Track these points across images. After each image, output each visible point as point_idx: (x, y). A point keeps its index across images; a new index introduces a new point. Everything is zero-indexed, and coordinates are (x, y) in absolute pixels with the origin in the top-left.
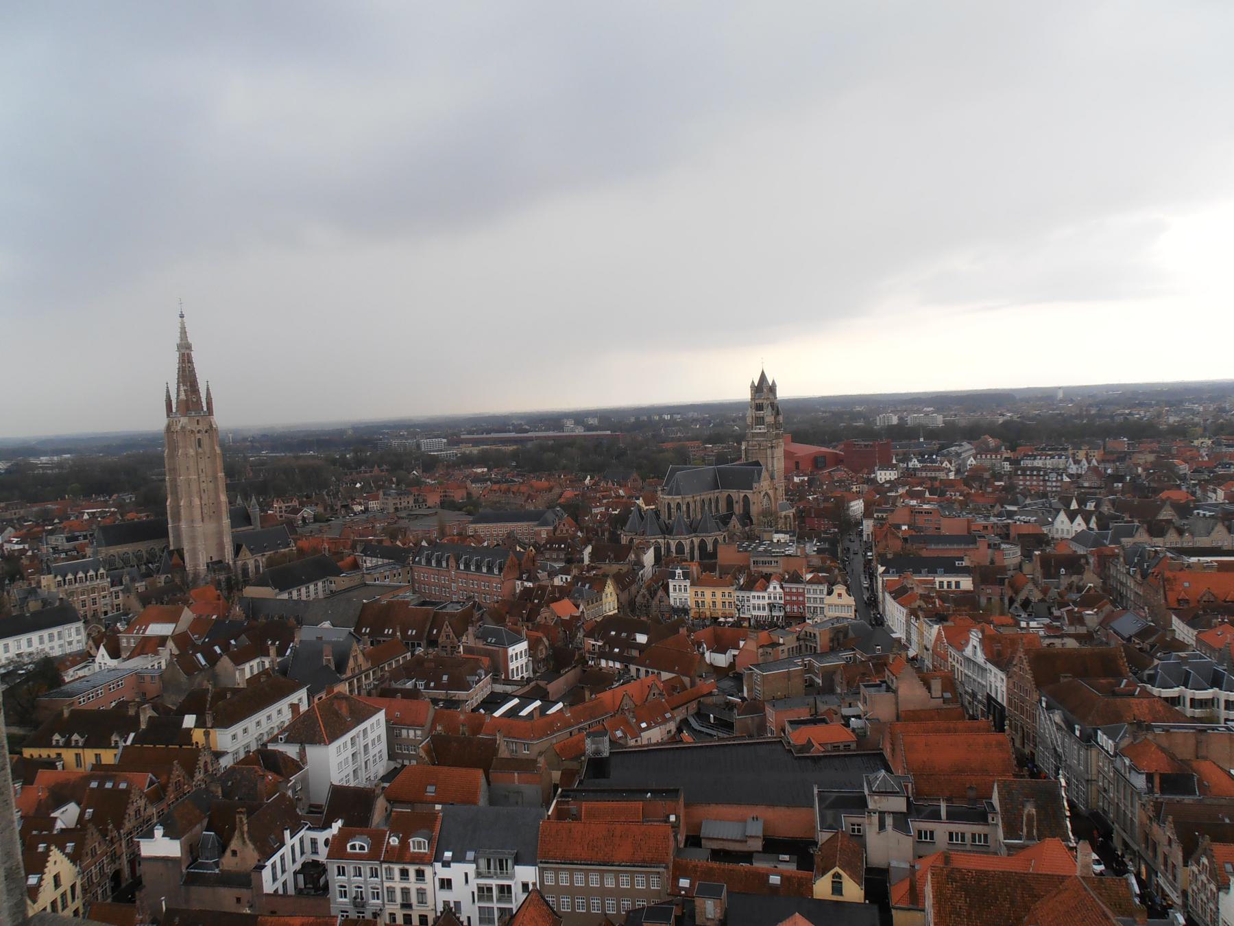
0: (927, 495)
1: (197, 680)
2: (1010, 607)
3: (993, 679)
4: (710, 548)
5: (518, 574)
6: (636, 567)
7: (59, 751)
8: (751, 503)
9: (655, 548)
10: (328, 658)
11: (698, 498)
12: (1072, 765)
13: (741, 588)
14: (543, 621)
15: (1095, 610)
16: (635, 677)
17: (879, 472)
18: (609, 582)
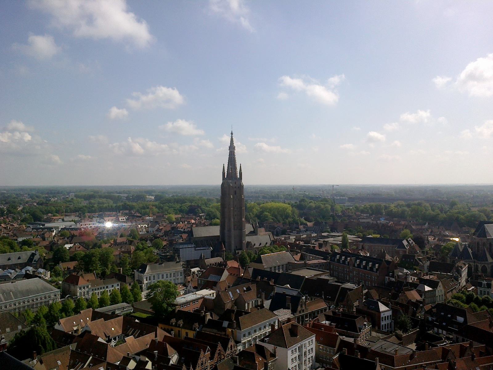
1: (229, 305)
7: (172, 327)
18: (440, 284)
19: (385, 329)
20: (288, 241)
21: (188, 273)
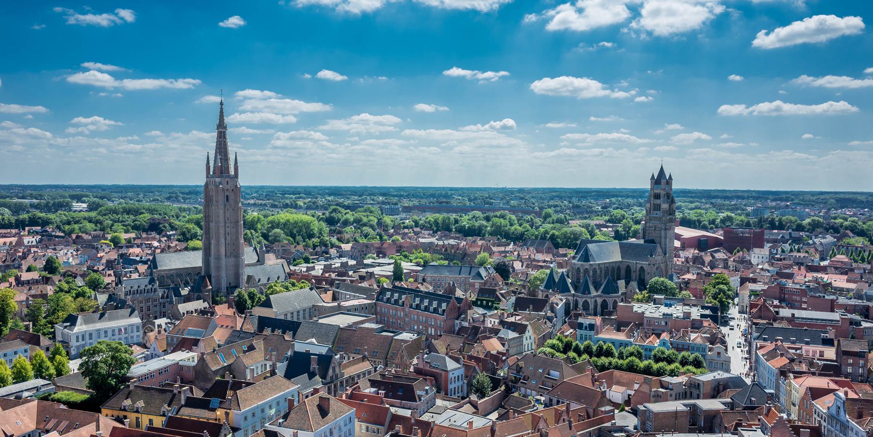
4: (610, 306)
5: (456, 315)
7: (125, 413)
8: (646, 273)
10: (314, 366)
11: (603, 266)
18: (529, 327)
19: (455, 394)
20: (313, 273)
21: (150, 327)
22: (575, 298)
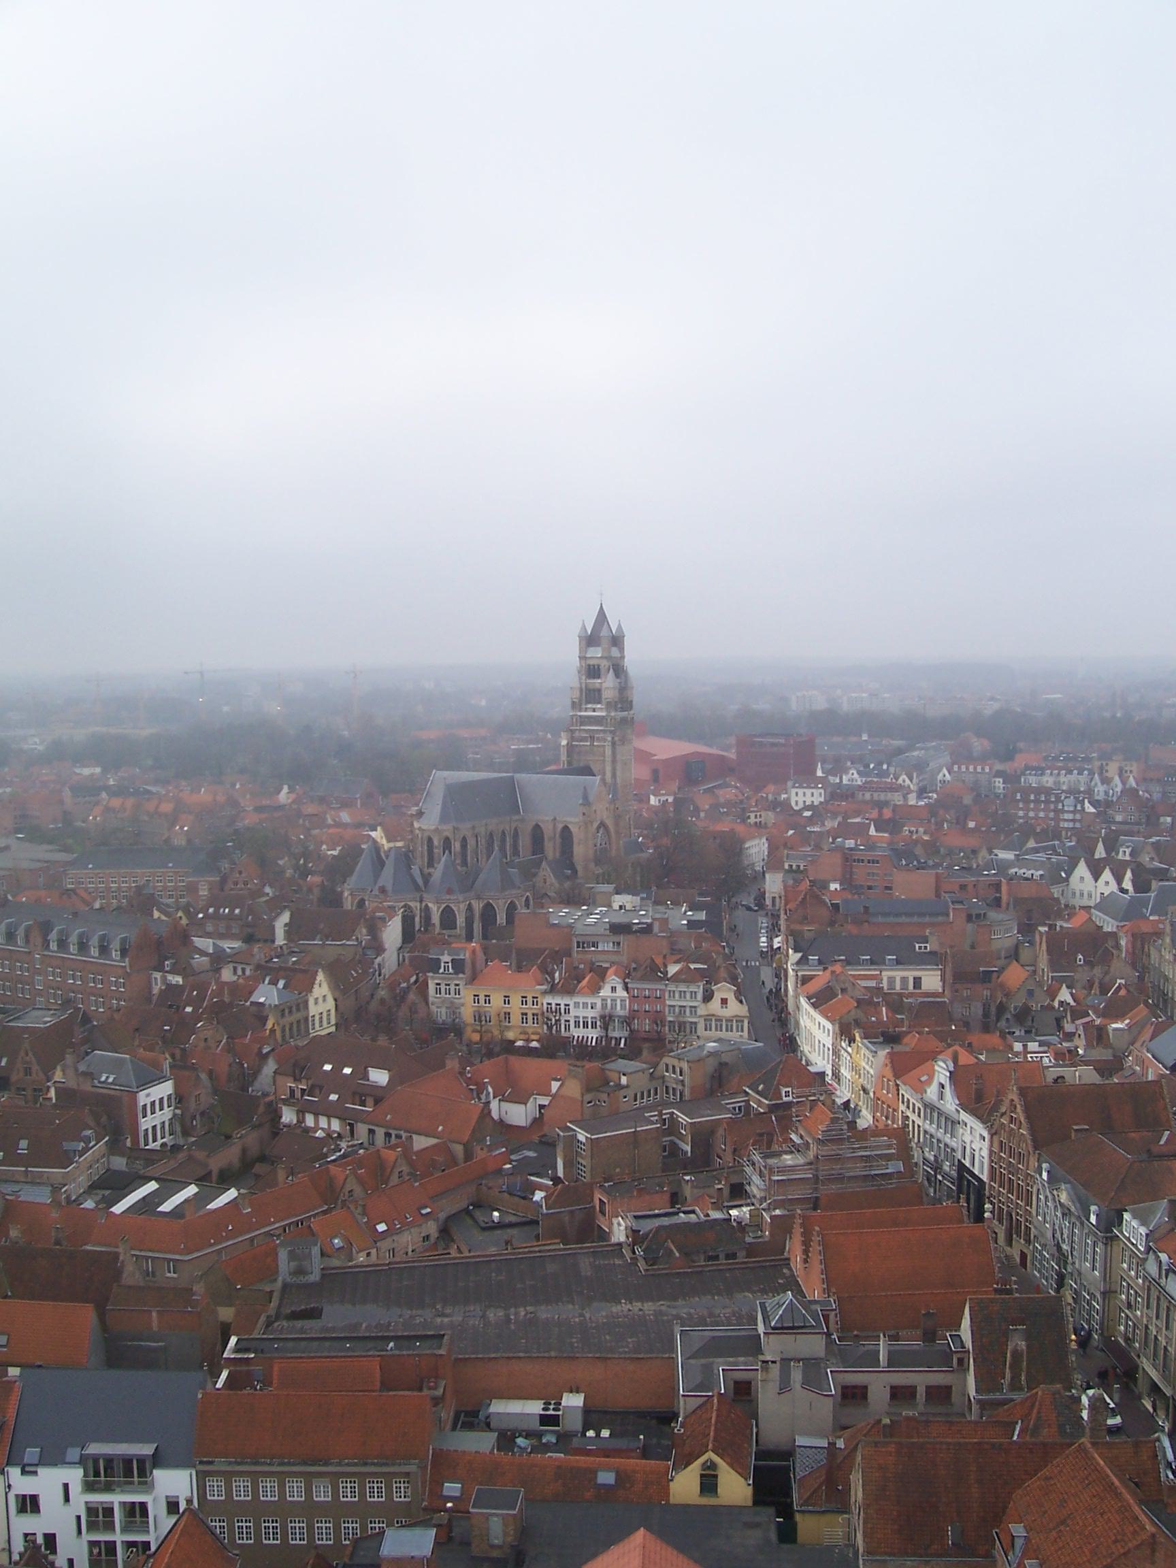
0: (872, 831)
2: (998, 1020)
3: (967, 1138)
4: (501, 919)
6: (369, 952)
8: (575, 840)
9: (403, 917)
11: (483, 830)
12: (1083, 1271)
13: (553, 990)
14: (202, 1044)
15: (1127, 1021)
16: (366, 1144)
17: (793, 791)
18: (320, 976)
22: (424, 904)
